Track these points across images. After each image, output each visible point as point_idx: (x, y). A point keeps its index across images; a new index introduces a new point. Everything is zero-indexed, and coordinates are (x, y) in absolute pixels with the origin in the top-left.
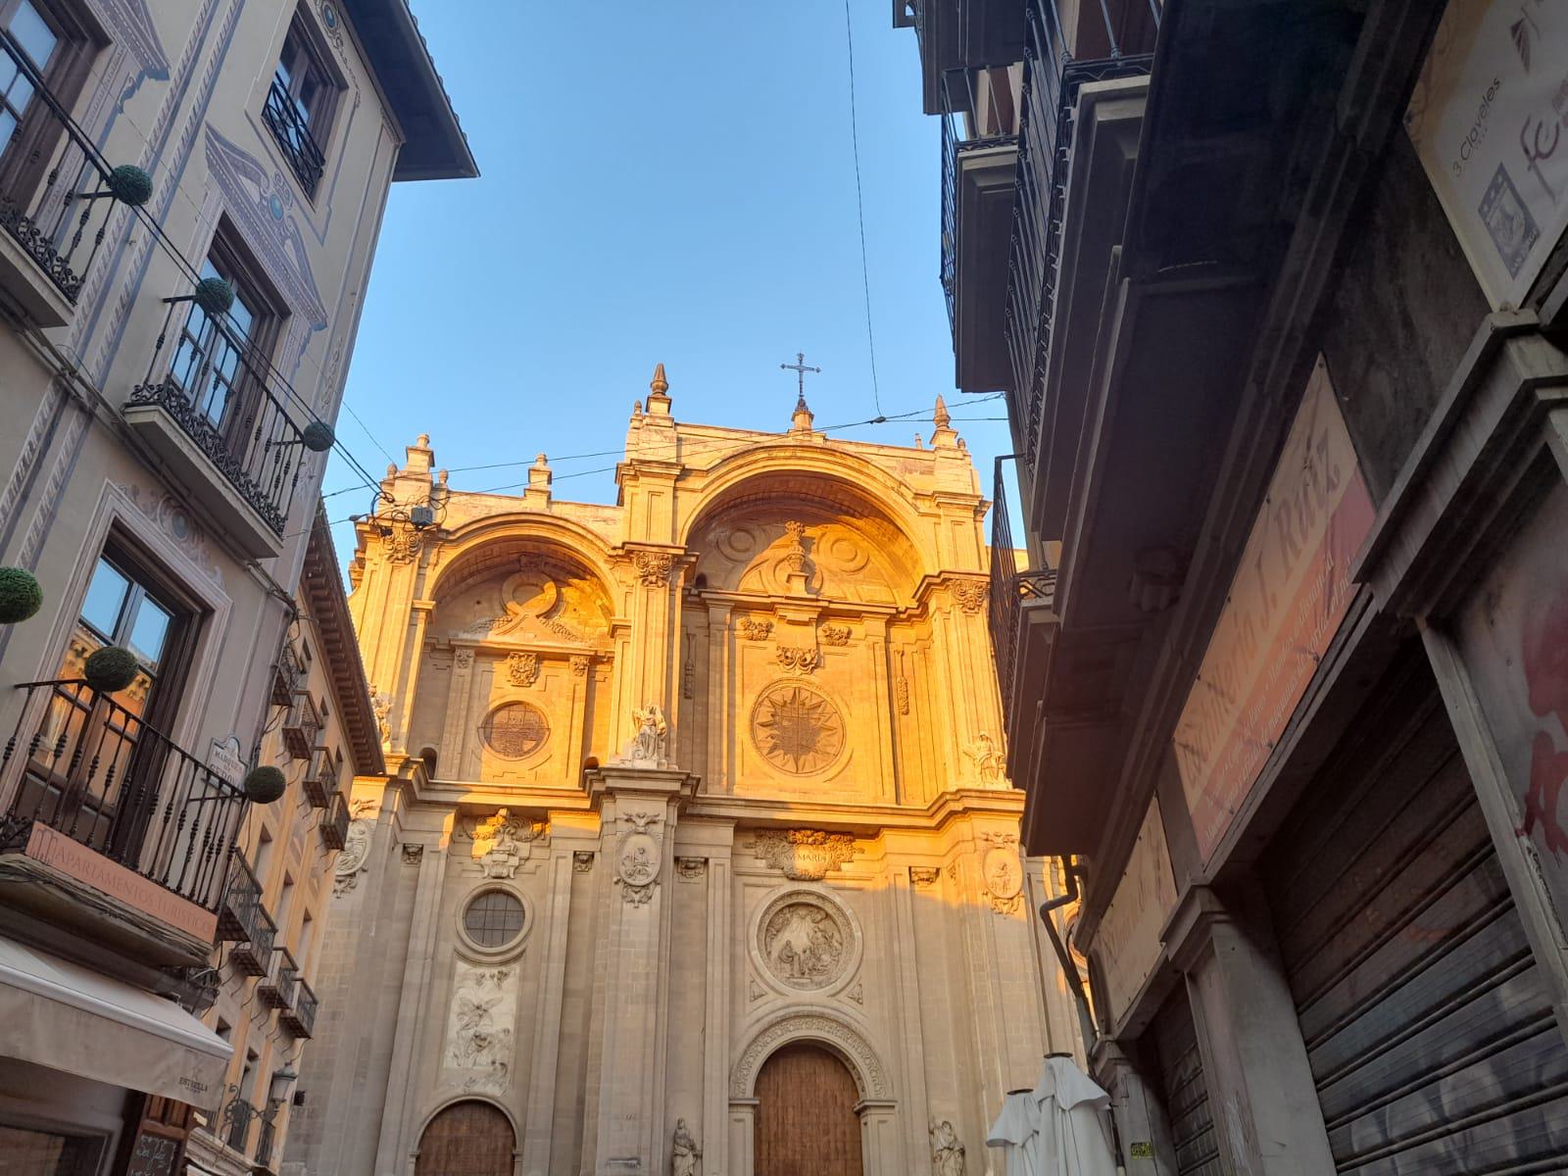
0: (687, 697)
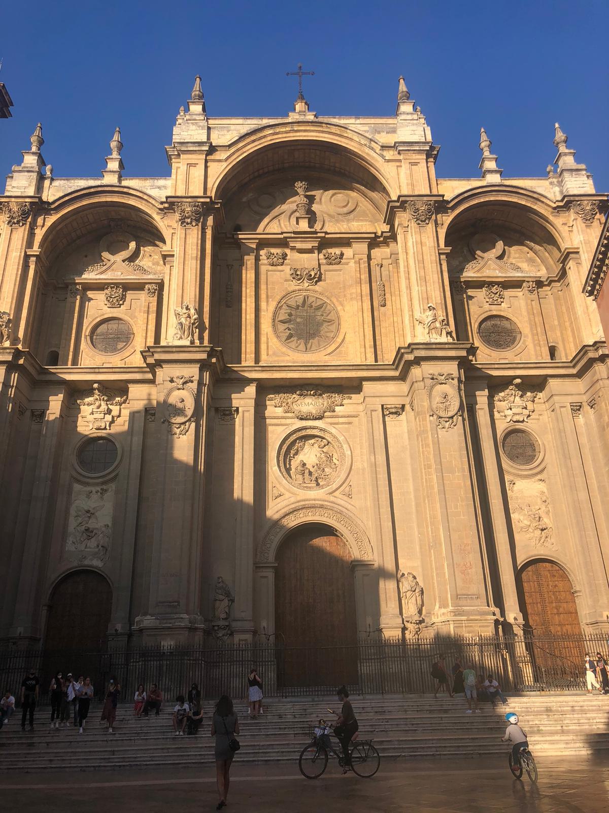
0: (228, 306)
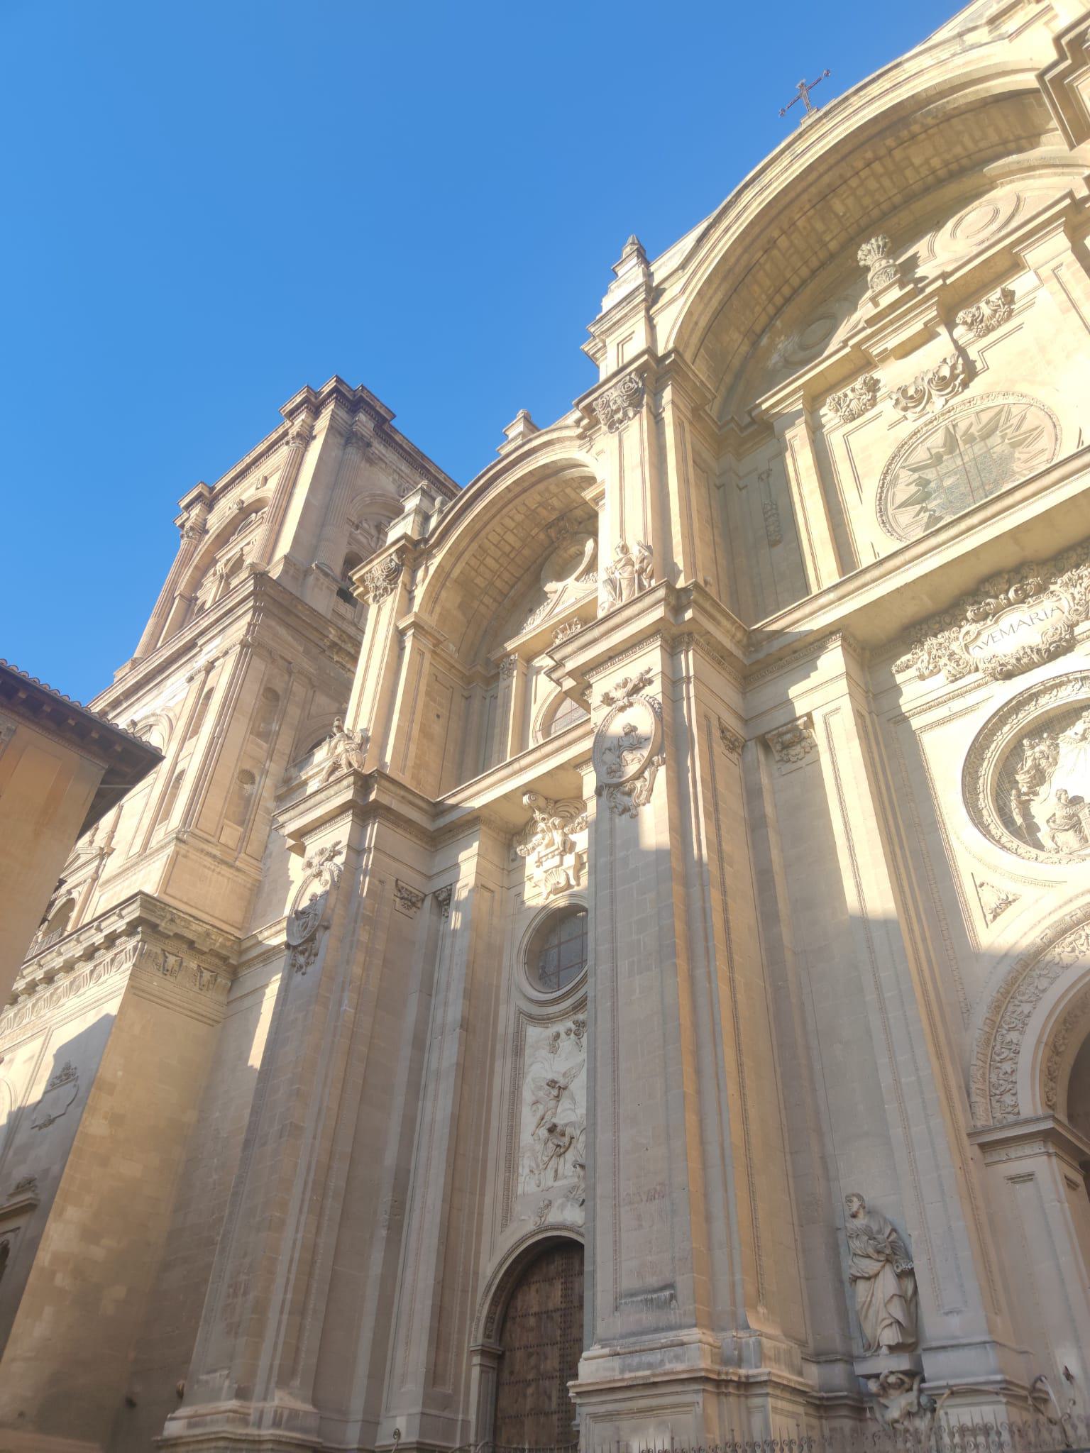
0: (773, 544)
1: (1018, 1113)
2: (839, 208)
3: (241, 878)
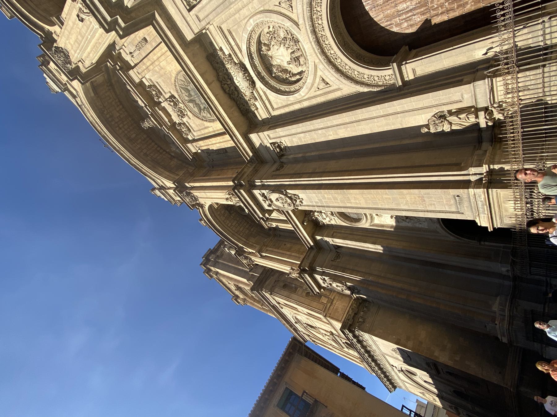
1: (392, 74)
2: (134, 135)
3: (337, 298)
